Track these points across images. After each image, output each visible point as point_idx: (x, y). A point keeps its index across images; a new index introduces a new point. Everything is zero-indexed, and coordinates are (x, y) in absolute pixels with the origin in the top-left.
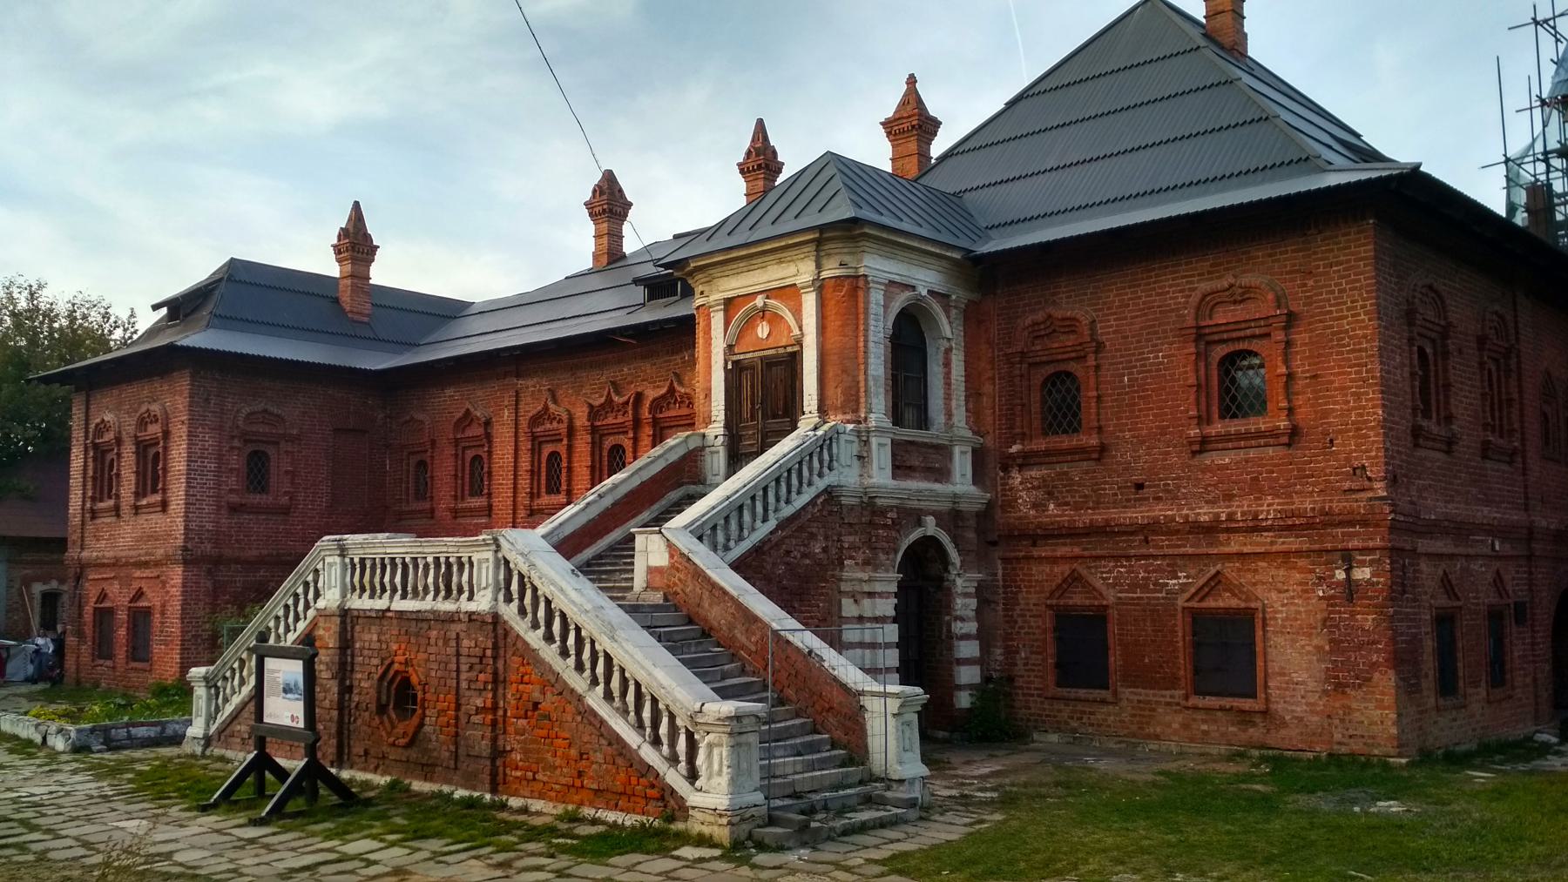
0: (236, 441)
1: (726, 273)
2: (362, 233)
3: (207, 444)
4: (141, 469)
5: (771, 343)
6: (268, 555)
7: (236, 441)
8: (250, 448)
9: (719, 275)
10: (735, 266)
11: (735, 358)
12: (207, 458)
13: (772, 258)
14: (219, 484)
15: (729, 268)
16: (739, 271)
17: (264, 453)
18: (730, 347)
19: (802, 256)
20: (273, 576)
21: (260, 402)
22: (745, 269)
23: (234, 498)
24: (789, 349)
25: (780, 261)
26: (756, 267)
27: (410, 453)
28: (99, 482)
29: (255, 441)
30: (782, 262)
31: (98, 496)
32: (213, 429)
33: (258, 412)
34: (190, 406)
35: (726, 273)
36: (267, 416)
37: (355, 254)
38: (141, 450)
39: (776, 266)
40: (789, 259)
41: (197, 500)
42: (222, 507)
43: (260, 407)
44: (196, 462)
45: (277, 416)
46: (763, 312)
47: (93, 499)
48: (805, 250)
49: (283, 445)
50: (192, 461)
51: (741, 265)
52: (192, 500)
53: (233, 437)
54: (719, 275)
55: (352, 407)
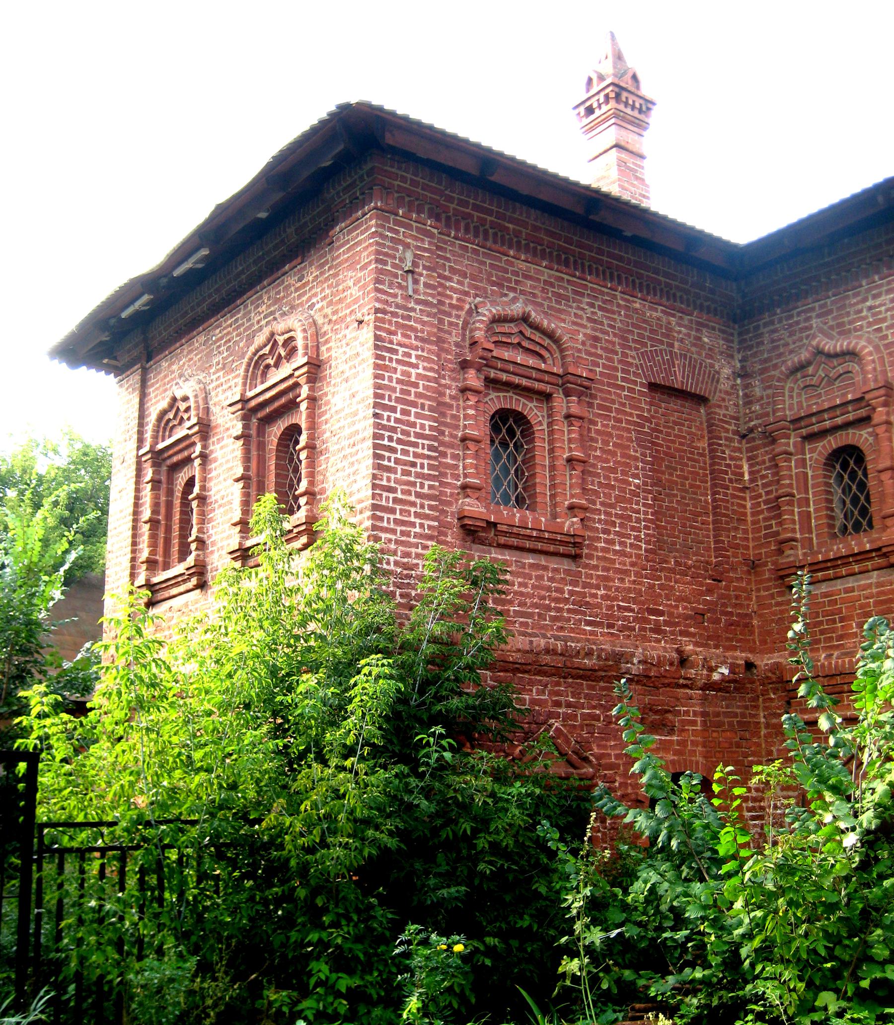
0: (472, 373)
2: (630, 74)
3: (413, 371)
4: (252, 473)
6: (547, 651)
7: (472, 373)
8: (497, 401)
12: (414, 404)
14: (440, 472)
17: (520, 418)
20: (558, 704)
21: (514, 300)
23: (473, 507)
27: (811, 437)
28: (162, 529)
29: (508, 386)
31: (159, 558)
32: (422, 340)
33: (512, 320)
34: (378, 281)
36: (528, 332)
37: (621, 107)
38: (253, 432)
41: (396, 500)
42: (448, 526)
43: (517, 308)
44: (393, 409)
45: (550, 335)
47: (151, 564)
49: (560, 403)
50: (385, 407)
52: (387, 499)
53: (464, 365)
55: (676, 344)
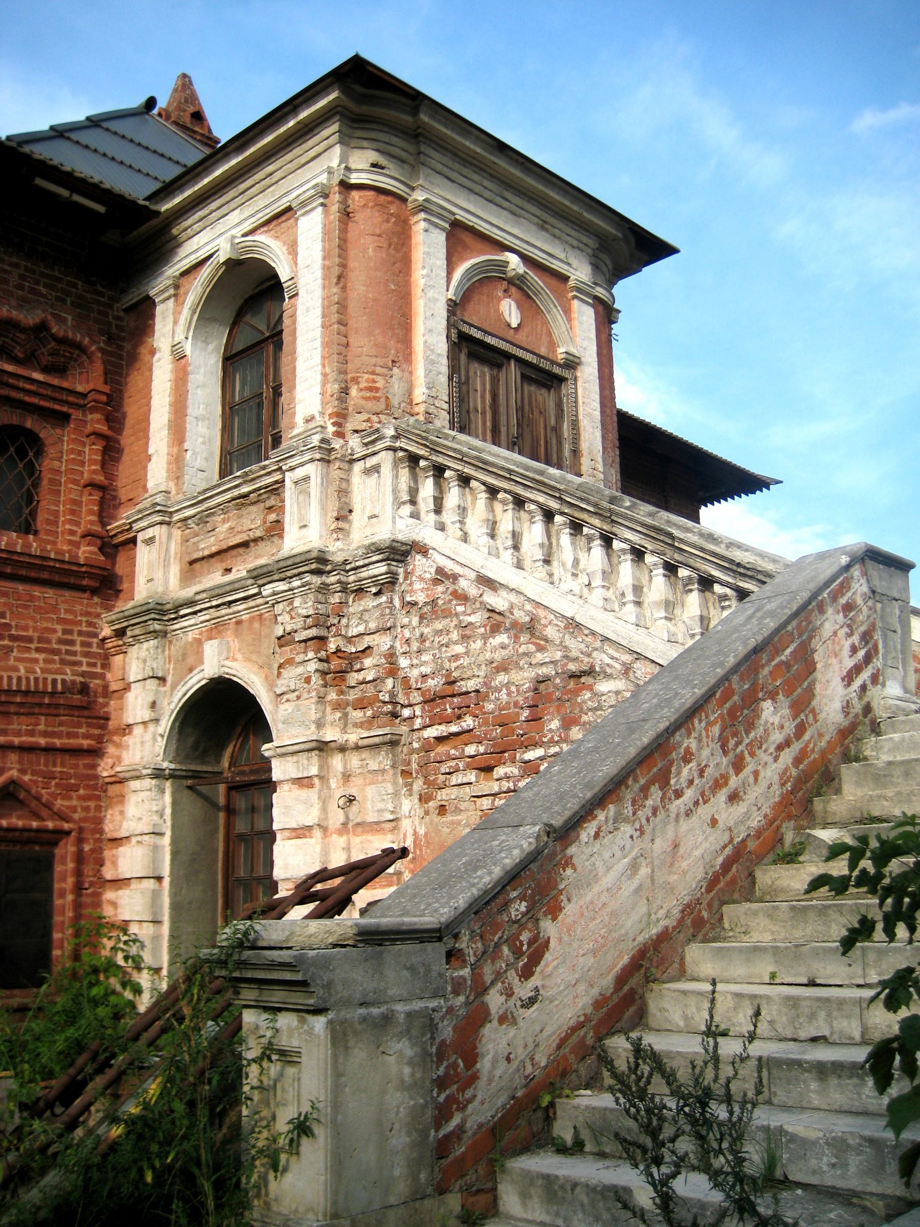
1: (454, 175)
5: (521, 338)
9: (439, 167)
10: (476, 177)
11: (465, 329)
13: (538, 212)
15: (465, 171)
16: (477, 188)
18: (454, 307)
19: (575, 243)
22: (487, 194)
24: (557, 370)
25: (543, 226)
26: (506, 204)
30: (542, 228)
35: (454, 175)
39: (534, 228)
40: (557, 232)
46: (517, 285)
48: (585, 239)
51: (486, 183)
54: (439, 167)
